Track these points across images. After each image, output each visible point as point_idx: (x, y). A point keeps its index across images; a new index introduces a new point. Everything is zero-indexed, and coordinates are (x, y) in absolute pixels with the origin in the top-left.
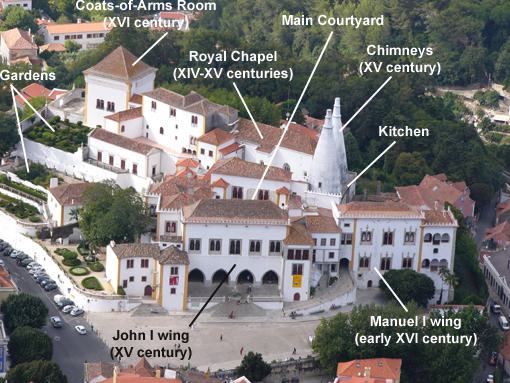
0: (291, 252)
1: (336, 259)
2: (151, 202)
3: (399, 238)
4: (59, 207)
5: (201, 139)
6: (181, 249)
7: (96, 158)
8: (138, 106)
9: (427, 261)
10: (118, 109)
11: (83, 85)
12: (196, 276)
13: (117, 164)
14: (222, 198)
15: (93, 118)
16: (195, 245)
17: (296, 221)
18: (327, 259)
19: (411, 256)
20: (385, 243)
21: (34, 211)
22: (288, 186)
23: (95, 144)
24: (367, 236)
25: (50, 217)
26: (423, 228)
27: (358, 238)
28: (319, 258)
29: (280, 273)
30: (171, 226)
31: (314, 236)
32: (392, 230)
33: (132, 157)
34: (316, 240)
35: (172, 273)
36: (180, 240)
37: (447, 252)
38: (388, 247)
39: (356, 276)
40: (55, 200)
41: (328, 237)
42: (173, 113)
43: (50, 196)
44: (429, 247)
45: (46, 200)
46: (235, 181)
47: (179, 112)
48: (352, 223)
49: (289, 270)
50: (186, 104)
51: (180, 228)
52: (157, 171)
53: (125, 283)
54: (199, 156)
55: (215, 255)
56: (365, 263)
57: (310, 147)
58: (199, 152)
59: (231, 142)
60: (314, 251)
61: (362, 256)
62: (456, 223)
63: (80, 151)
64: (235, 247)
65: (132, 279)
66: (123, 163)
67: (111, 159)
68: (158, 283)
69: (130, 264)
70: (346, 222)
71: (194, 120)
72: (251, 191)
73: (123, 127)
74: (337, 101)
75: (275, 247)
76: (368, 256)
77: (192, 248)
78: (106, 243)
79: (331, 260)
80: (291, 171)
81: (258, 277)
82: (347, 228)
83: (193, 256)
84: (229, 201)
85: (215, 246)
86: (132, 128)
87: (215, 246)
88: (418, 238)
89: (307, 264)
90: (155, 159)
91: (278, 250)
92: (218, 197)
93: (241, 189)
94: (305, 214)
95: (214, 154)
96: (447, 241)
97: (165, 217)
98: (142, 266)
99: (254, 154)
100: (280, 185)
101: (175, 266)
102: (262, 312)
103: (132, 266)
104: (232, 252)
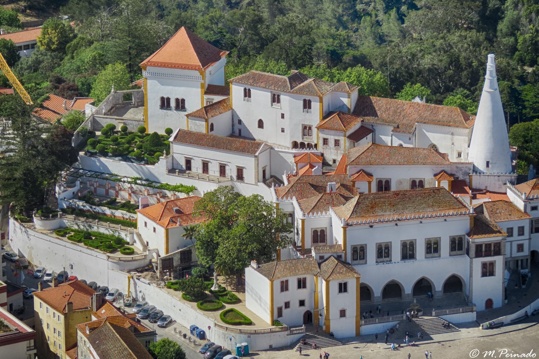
0: (479, 247)
1: (526, 252)
6: (343, 259)
7: (184, 167)
8: (217, 98)
12: (365, 292)
15: (158, 122)
16: (359, 253)
18: (515, 254)
21: (120, 242)
23: (180, 151)
25: (146, 246)
30: (320, 237)
33: (234, 160)
40: (151, 224)
42: (276, 99)
52: (268, 176)
53: (280, 310)
54: (321, 148)
58: (321, 142)
64: (408, 252)
65: (287, 305)
69: (284, 287)
71: (307, 105)
72: (400, 182)
73: (212, 125)
79: (521, 254)
85: (384, 252)
86: (221, 121)
89: (499, 261)
93: (388, 182)
95: (342, 143)
103: (287, 289)
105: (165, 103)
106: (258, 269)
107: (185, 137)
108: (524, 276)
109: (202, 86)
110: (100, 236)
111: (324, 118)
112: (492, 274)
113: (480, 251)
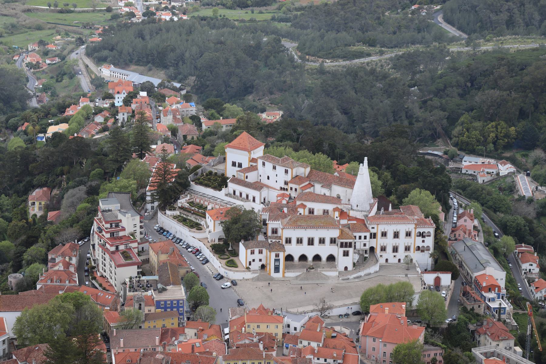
0: (342, 243)
1: (367, 247)
2: (263, 217)
3: (402, 235)
4: (212, 221)
5: (291, 182)
8: (254, 164)
9: (419, 247)
10: (243, 167)
11: (224, 153)
12: (289, 258)
13: (244, 196)
14: (302, 214)
15: (231, 172)
16: (289, 241)
17: (344, 226)
18: (362, 247)
19: (409, 245)
20: (395, 237)
22: (340, 207)
24: (384, 234)
26: (415, 228)
27: (379, 235)
28: (358, 247)
29: (336, 256)
30: (275, 231)
31: (355, 234)
32: (398, 230)
33: (252, 193)
34: (355, 237)
35: (276, 256)
36: (280, 238)
37: (430, 242)
38: (396, 239)
39: (379, 256)
40: (210, 218)
41: (363, 235)
42: (274, 168)
43: (207, 215)
44: (420, 239)
45: (205, 218)
46: (310, 205)
47: (277, 167)
48: (375, 226)
49: (341, 253)
50: (282, 163)
51: (280, 231)
55: (300, 246)
56: (383, 249)
57: (350, 184)
58: (289, 189)
59: (308, 183)
60: (355, 243)
61: (382, 245)
62: (434, 225)
63: (224, 190)
65: (254, 260)
66: (247, 196)
67: (241, 194)
68: (268, 262)
69: (253, 253)
70: (373, 226)
71: (286, 172)
72: (318, 210)
74: (366, 158)
75: (333, 241)
76: (385, 245)
77: (286, 242)
78: (240, 241)
80: (341, 198)
81: (324, 258)
82: (373, 229)
83: (287, 247)
84: (308, 216)
85: (300, 241)
87: (300, 241)
88: (413, 234)
89: (351, 250)
90: (265, 192)
91: (335, 242)
92: (300, 214)
93: (313, 209)
94: (349, 222)
96: (429, 236)
97: (272, 225)
98: (259, 253)
99: (318, 189)
100: (335, 206)
101: (277, 253)
102: (328, 278)
103: (254, 253)
104: (309, 244)
105: (234, 164)
106: (243, 244)
107: (236, 181)
108: (366, 258)
109: (249, 158)
110: (191, 221)
111: (292, 178)
112: (347, 255)
113: (342, 245)
